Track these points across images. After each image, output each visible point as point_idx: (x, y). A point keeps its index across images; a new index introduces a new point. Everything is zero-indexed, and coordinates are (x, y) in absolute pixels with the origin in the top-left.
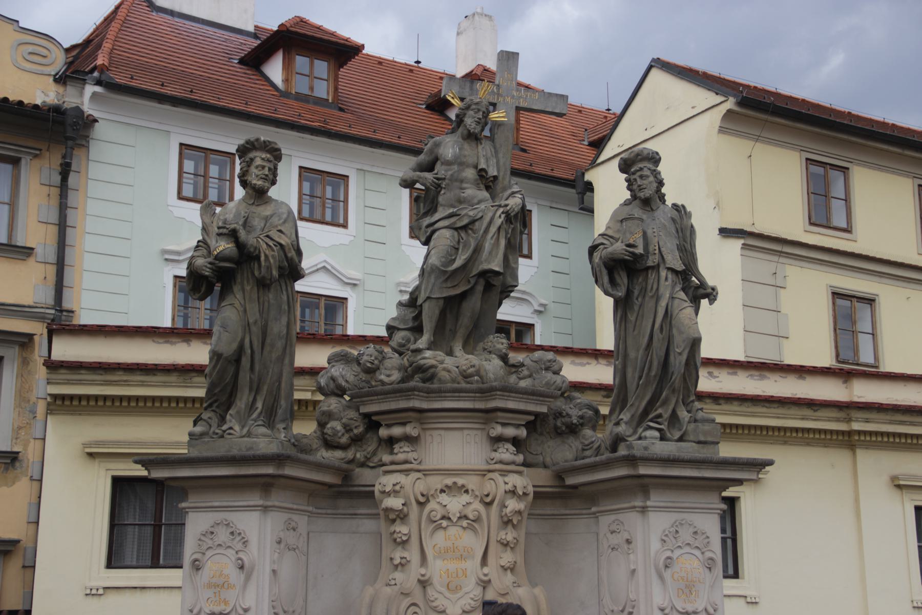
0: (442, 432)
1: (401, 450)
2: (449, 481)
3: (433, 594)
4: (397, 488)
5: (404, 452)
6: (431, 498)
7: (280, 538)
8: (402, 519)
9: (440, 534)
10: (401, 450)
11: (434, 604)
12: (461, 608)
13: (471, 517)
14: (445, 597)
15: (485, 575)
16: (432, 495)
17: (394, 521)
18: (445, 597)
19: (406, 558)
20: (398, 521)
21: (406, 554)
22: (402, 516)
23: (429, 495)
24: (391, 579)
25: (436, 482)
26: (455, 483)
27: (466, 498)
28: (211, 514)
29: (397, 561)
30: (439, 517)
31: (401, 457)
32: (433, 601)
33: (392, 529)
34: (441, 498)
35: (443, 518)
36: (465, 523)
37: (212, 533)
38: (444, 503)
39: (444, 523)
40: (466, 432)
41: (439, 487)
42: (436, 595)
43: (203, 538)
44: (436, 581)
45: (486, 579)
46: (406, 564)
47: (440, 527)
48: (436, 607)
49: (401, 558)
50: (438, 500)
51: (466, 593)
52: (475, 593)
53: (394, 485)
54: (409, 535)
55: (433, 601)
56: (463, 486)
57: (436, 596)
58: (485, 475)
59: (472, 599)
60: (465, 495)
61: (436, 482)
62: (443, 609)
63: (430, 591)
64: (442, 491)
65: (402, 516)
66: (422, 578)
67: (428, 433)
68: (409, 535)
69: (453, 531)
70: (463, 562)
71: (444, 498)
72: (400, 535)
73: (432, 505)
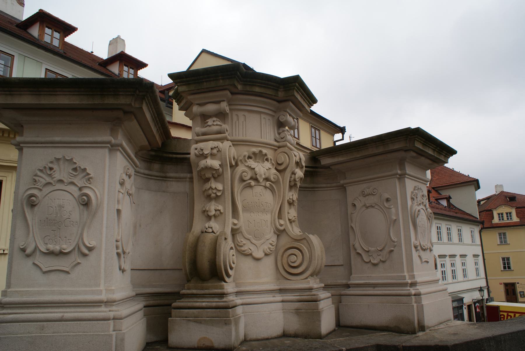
0: (246, 114)
1: (215, 123)
2: (256, 150)
3: (242, 240)
4: (215, 151)
5: (217, 125)
6: (239, 163)
7: (123, 179)
8: (215, 178)
9: (248, 191)
10: (215, 123)
11: (243, 249)
12: (264, 252)
13: (272, 179)
14: (251, 243)
15: (281, 225)
16: (241, 160)
17: (208, 180)
18: (251, 243)
19: (219, 210)
20: (212, 180)
21: (220, 208)
22: (217, 175)
23: (239, 160)
24: (207, 227)
25: (245, 151)
26: (261, 152)
27: (268, 165)
28: (50, 151)
29: (213, 213)
30: (249, 177)
31: (215, 128)
32: (242, 246)
33: (207, 186)
34: (249, 163)
35: (251, 178)
36: (268, 184)
37: (51, 169)
38: (253, 167)
39: (253, 183)
40: (263, 116)
41: (247, 154)
42: (244, 241)
43: (39, 173)
44: (243, 229)
45: (282, 228)
46: (219, 216)
47: (250, 186)
48: (244, 251)
49: (216, 210)
50: (247, 164)
51: (267, 240)
52: (272, 240)
53: (212, 149)
54: (223, 191)
55: (242, 246)
56: (266, 155)
57: (244, 242)
58: (276, 150)
59: (271, 244)
60: (266, 162)
61: (245, 151)
62: (250, 252)
63: (239, 238)
64: (250, 157)
65: (217, 175)
66: (235, 227)
67: (234, 113)
68: (223, 191)
69: (259, 189)
70: (265, 215)
71: (252, 163)
72: (214, 191)
73: (241, 168)
